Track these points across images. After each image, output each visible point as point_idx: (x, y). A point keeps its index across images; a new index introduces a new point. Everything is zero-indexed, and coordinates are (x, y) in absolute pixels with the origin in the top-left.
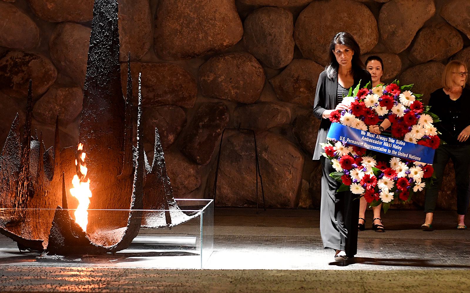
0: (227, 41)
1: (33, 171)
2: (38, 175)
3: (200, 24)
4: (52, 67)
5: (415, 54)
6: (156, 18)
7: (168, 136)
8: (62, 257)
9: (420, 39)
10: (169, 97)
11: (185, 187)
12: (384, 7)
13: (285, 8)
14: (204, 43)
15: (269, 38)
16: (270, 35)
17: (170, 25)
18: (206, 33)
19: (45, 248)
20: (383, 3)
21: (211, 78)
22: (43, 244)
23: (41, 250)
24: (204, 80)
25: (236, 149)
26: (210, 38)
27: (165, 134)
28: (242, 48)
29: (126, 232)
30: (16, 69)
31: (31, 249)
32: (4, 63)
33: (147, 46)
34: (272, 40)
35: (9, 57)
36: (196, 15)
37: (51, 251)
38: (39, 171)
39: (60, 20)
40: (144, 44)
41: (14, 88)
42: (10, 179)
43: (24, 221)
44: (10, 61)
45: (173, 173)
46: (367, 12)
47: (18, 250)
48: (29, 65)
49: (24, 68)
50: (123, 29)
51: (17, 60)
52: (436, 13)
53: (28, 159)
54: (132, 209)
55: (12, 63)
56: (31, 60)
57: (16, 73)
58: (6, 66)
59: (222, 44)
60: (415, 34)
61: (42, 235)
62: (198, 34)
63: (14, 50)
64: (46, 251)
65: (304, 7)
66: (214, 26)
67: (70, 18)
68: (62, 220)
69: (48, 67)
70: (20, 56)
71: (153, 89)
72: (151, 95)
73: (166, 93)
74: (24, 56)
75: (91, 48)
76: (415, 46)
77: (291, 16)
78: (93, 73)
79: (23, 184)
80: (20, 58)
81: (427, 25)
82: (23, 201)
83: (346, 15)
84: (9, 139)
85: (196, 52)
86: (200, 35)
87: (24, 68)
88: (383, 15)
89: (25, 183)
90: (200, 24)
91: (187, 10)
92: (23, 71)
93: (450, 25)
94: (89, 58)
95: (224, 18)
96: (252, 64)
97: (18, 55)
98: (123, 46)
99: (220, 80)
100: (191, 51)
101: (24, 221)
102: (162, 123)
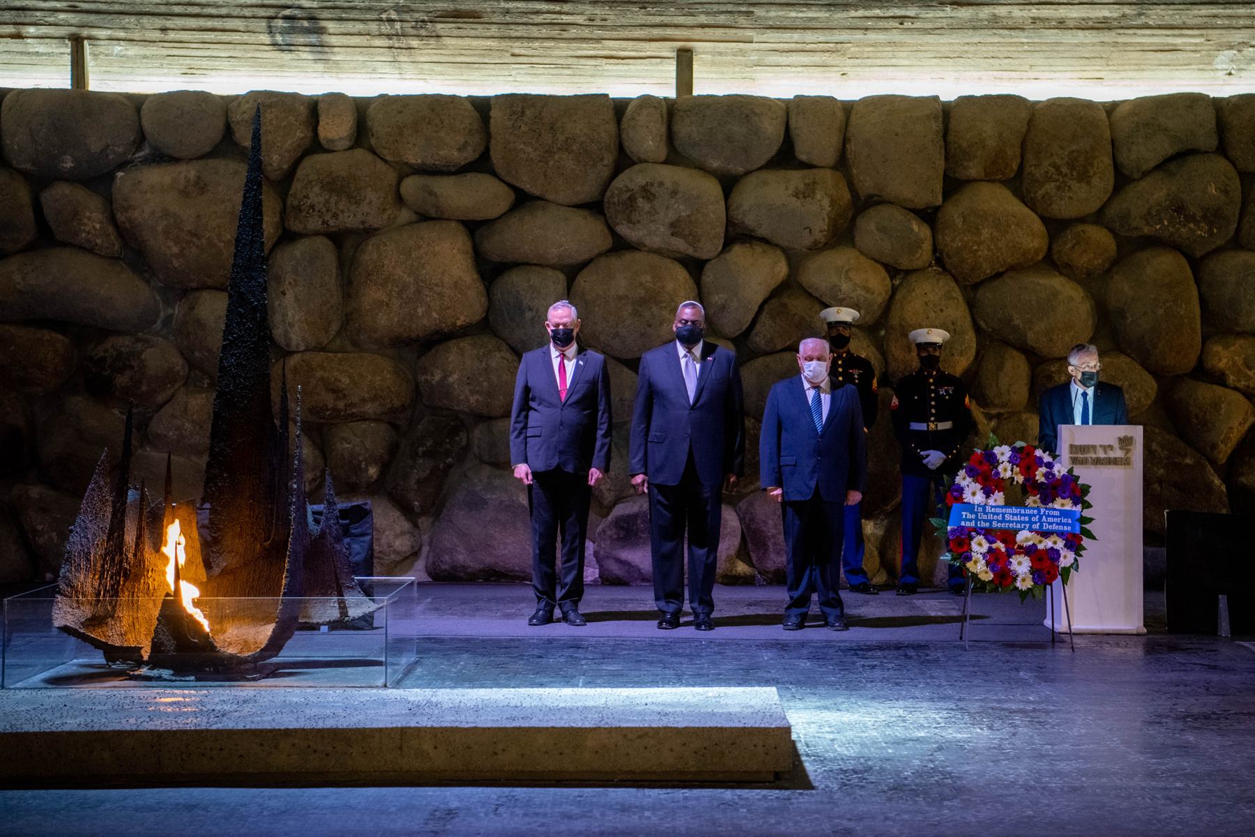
0: (462, 318)
1: (130, 538)
2: (137, 545)
3: (419, 291)
4: (181, 361)
5: (757, 339)
6: (350, 283)
7: (367, 470)
9: (764, 317)
10: (370, 408)
12: (708, 266)
13: (553, 267)
14: (425, 322)
15: (528, 315)
16: (530, 309)
17: (372, 295)
18: (429, 307)
19: (146, 658)
20: (707, 261)
21: (437, 378)
22: (143, 652)
23: (140, 663)
24: (426, 380)
25: (478, 489)
26: (435, 315)
28: (485, 326)
29: (274, 631)
31: (121, 663)
33: (335, 327)
34: (533, 318)
36: (412, 280)
37: (154, 663)
38: (139, 537)
39: (194, 285)
40: (330, 323)
42: (92, 552)
43: (113, 617)
46: (681, 274)
47: (103, 661)
50: (297, 300)
52: (789, 276)
53: (123, 521)
54: (284, 595)
59: (454, 324)
60: (756, 309)
61: (143, 637)
62: (415, 309)
64: (147, 663)
65: (584, 265)
66: (441, 295)
67: (210, 282)
68: (171, 615)
69: (174, 360)
71: (345, 396)
72: (341, 405)
73: (364, 400)
75: (224, 347)
76: (758, 327)
77: (562, 277)
78: (227, 386)
79: (113, 560)
81: (776, 293)
82: (112, 586)
83: (648, 278)
84: (93, 490)
85: (413, 335)
86: (420, 310)
88: (708, 277)
89: (117, 558)
90: (419, 291)
91: (399, 271)
93: (810, 295)
94: (221, 361)
95: (456, 284)
96: (502, 354)
99: (451, 380)
100: (405, 335)
101: (113, 617)
102: (357, 449)
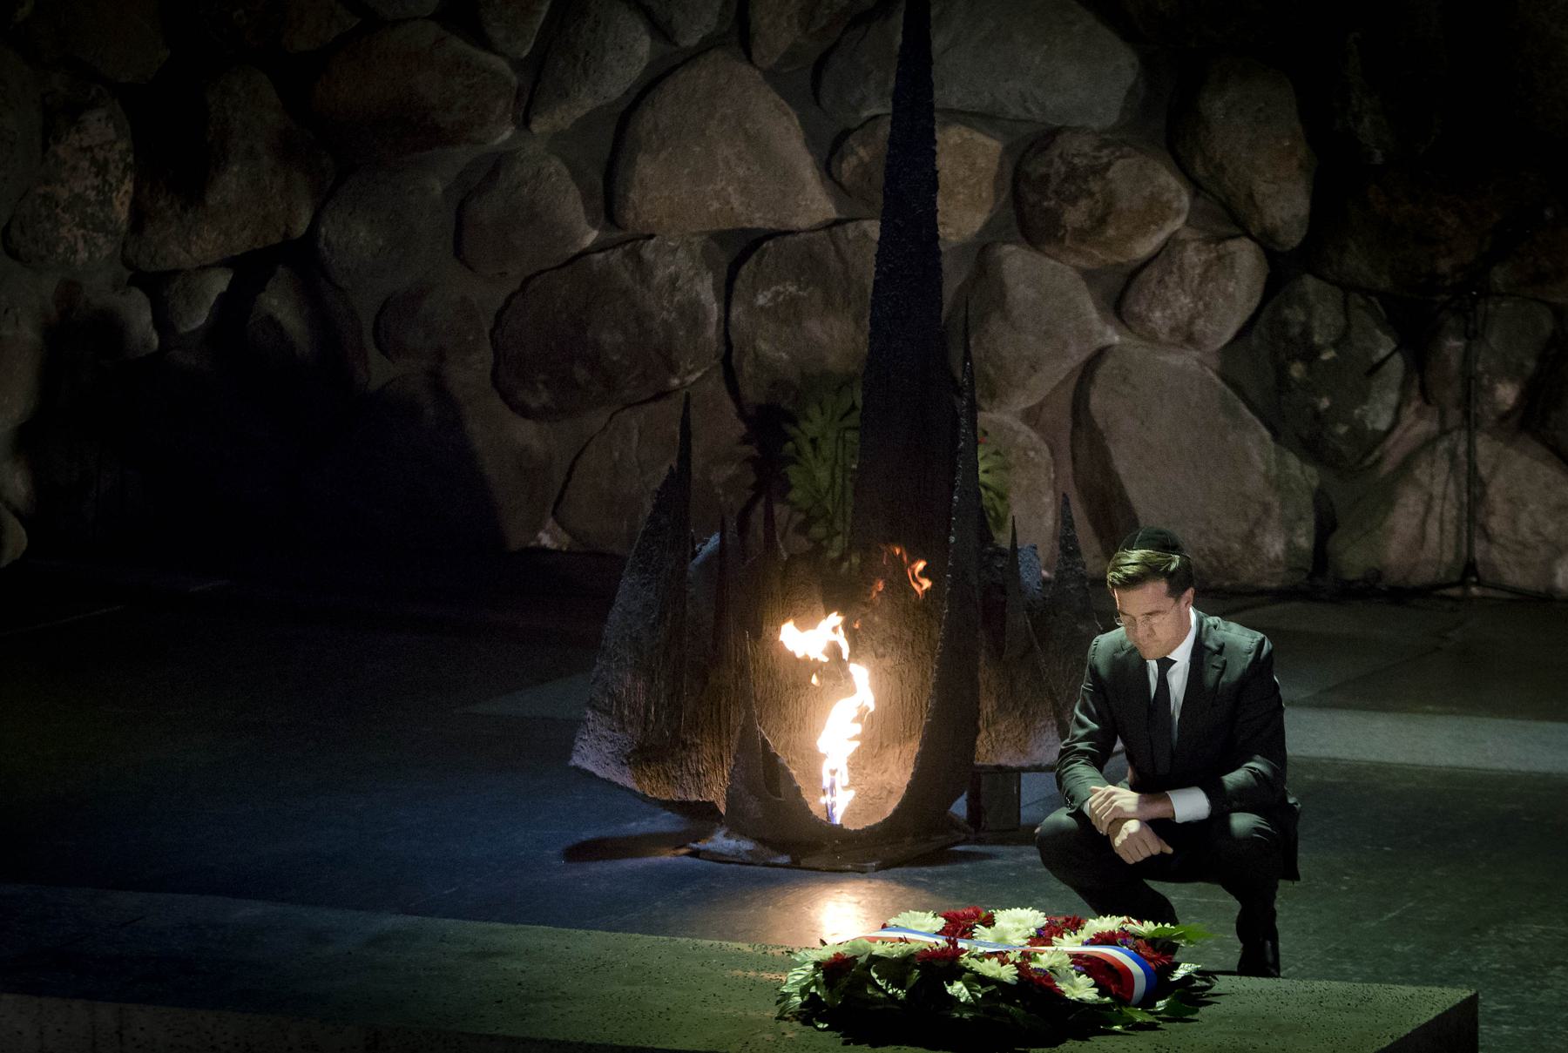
7: (1491, 390)
8: (747, 845)
11: (1546, 541)
27: (1485, 382)
30: (1073, 188)
32: (1043, 170)
35: (1057, 152)
41: (1067, 242)
44: (1057, 162)
45: (1510, 501)
48: (1110, 174)
49: (1095, 186)
51: (1076, 161)
55: (1063, 169)
56: (1118, 158)
57: (1073, 200)
58: (1045, 178)
63: (1076, 131)
70: (1087, 149)
74: (1099, 148)
80: (1085, 155)
87: (1095, 186)
92: (1091, 194)
97: (1079, 148)
98: (1366, 120)
